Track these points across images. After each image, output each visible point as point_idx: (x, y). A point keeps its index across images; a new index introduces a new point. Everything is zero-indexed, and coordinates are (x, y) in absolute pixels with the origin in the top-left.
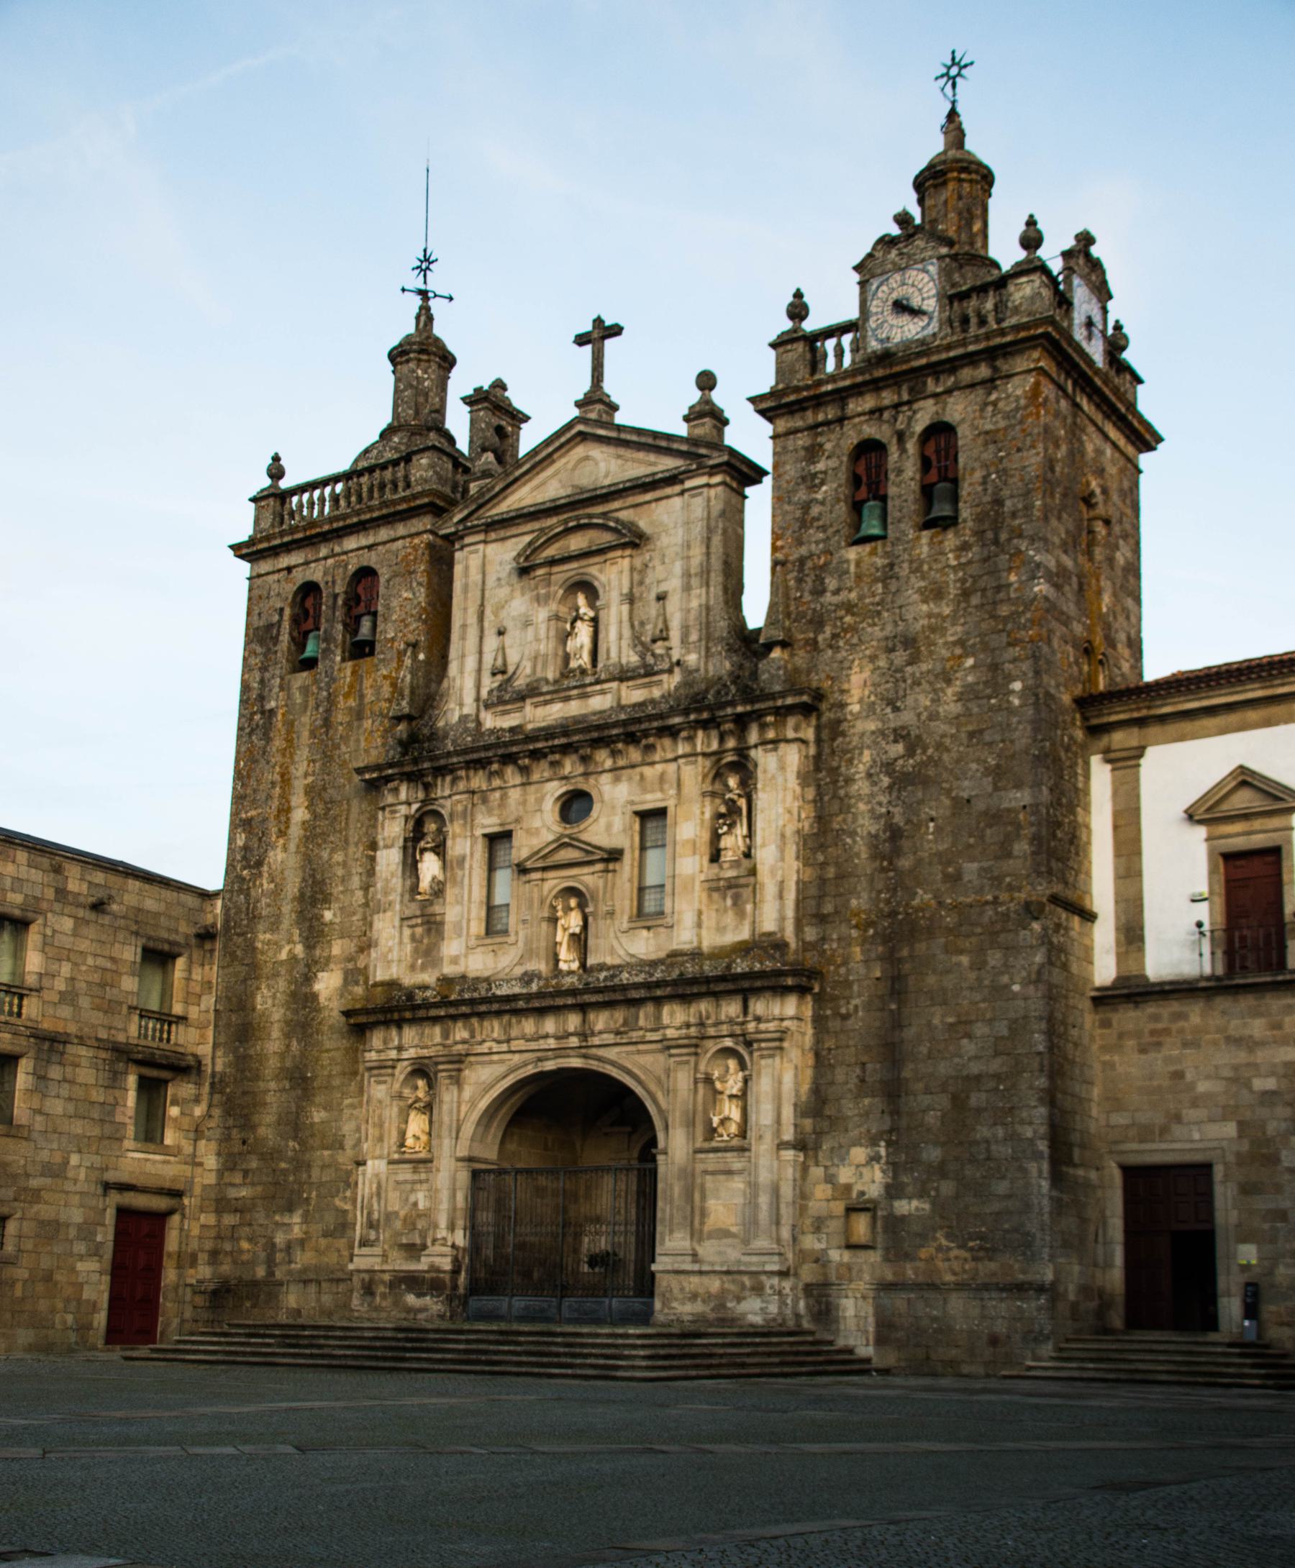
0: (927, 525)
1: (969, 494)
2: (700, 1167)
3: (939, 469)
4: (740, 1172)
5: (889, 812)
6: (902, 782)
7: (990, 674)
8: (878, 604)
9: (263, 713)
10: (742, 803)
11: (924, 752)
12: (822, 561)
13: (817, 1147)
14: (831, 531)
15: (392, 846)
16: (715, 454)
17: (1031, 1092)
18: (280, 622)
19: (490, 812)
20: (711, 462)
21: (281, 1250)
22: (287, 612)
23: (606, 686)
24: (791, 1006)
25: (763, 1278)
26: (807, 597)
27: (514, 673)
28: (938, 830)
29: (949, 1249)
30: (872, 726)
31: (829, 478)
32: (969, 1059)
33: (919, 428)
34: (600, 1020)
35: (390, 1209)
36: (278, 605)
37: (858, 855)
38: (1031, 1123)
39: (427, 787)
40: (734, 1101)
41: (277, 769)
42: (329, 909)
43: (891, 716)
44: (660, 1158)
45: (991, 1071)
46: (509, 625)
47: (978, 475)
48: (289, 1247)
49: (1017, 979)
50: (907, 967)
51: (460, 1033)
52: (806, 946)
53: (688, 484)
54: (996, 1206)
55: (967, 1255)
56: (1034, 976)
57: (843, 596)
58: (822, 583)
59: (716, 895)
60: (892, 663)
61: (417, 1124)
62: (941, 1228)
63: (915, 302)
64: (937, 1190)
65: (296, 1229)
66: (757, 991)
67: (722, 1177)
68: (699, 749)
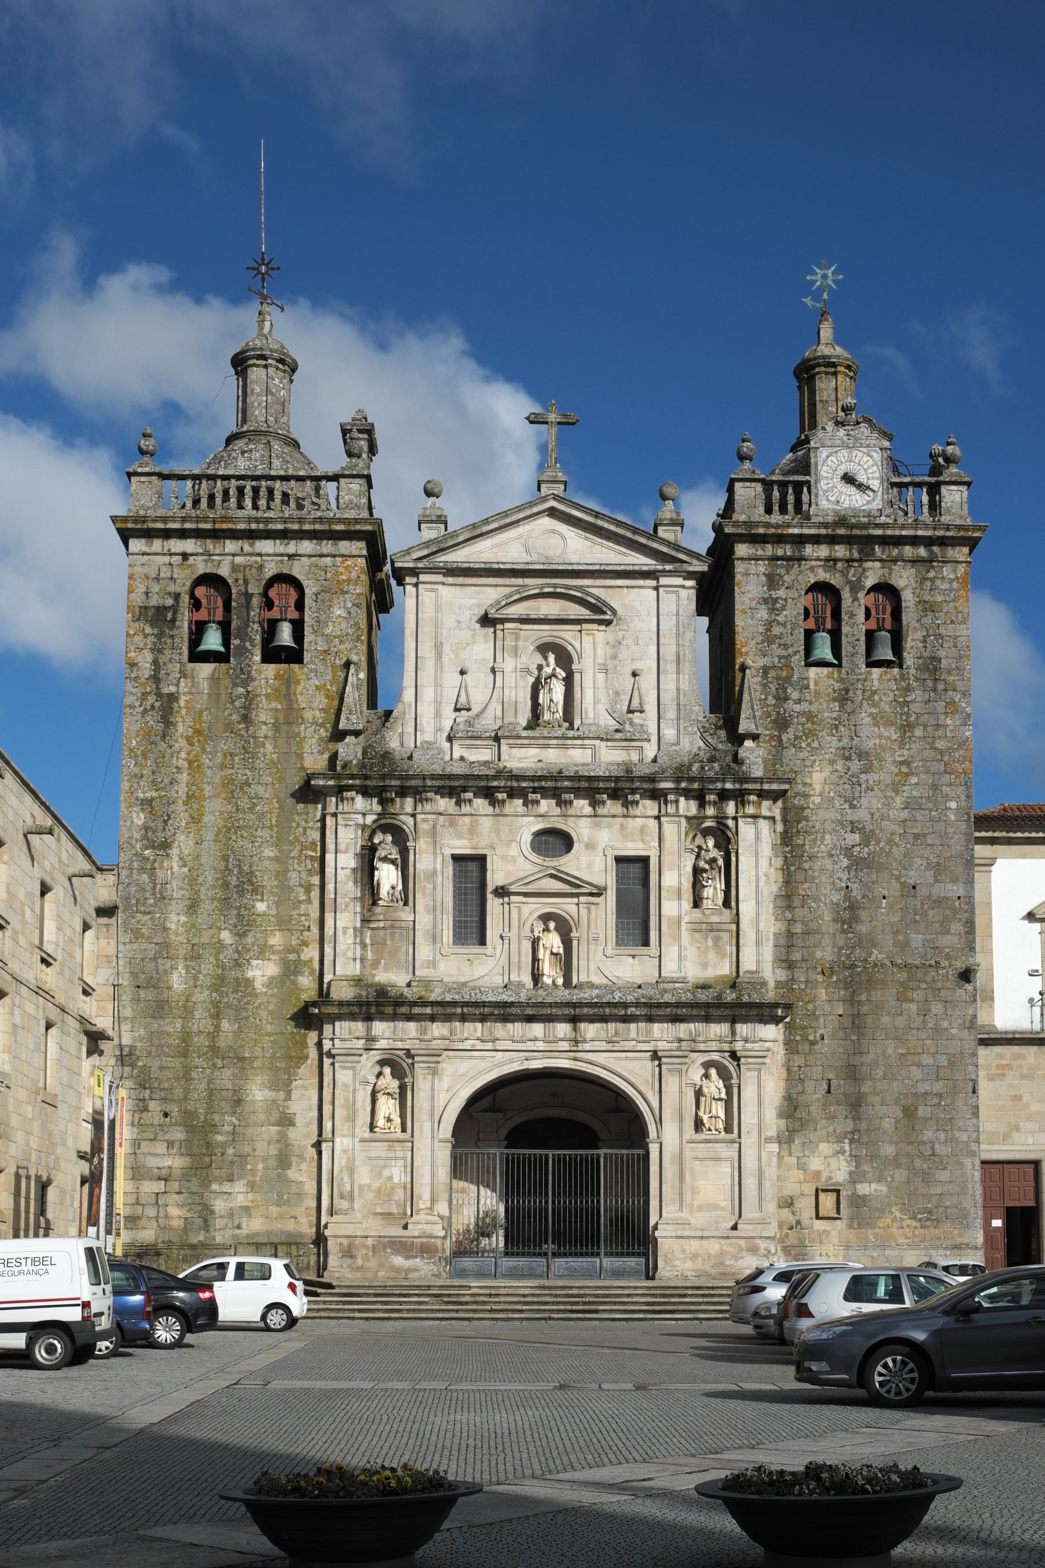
0: (870, 664)
1: (912, 647)
2: (688, 1155)
3: (878, 619)
4: (726, 1159)
5: (847, 887)
6: (857, 864)
7: (931, 792)
8: (835, 719)
9: (159, 695)
10: (721, 862)
11: (877, 843)
12: (784, 674)
13: (790, 1141)
14: (791, 650)
15: (346, 851)
16: (695, 562)
17: (965, 1108)
18: (175, 609)
19: (460, 836)
20: (691, 569)
21: (221, 1217)
22: (185, 599)
23: (586, 742)
24: (771, 1032)
25: (759, 1241)
26: (771, 700)
27: (482, 712)
28: (890, 906)
29: (902, 1220)
30: (832, 815)
31: (789, 606)
32: (917, 1081)
33: (869, 583)
34: (590, 1030)
35: (362, 1182)
36: (172, 588)
37: (821, 917)
38: (966, 1130)
39: (382, 802)
40: (719, 1103)
41: (183, 755)
42: (262, 900)
43: (848, 811)
44: (654, 1149)
45: (934, 1091)
46: (469, 666)
47: (919, 635)
48: (231, 1213)
49: (955, 1025)
50: (865, 1009)
51: (438, 1029)
52: (779, 984)
53: (663, 581)
54: (939, 1190)
55: (918, 1224)
56: (967, 1024)
57: (804, 707)
58: (785, 692)
59: (697, 935)
60: (849, 769)
61: (387, 1107)
62: (896, 1204)
63: (862, 478)
64: (892, 1176)
65: (240, 1198)
66: (745, 1020)
67: (711, 1163)
68: (681, 812)
